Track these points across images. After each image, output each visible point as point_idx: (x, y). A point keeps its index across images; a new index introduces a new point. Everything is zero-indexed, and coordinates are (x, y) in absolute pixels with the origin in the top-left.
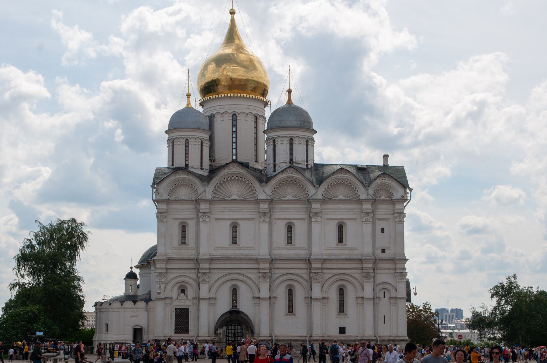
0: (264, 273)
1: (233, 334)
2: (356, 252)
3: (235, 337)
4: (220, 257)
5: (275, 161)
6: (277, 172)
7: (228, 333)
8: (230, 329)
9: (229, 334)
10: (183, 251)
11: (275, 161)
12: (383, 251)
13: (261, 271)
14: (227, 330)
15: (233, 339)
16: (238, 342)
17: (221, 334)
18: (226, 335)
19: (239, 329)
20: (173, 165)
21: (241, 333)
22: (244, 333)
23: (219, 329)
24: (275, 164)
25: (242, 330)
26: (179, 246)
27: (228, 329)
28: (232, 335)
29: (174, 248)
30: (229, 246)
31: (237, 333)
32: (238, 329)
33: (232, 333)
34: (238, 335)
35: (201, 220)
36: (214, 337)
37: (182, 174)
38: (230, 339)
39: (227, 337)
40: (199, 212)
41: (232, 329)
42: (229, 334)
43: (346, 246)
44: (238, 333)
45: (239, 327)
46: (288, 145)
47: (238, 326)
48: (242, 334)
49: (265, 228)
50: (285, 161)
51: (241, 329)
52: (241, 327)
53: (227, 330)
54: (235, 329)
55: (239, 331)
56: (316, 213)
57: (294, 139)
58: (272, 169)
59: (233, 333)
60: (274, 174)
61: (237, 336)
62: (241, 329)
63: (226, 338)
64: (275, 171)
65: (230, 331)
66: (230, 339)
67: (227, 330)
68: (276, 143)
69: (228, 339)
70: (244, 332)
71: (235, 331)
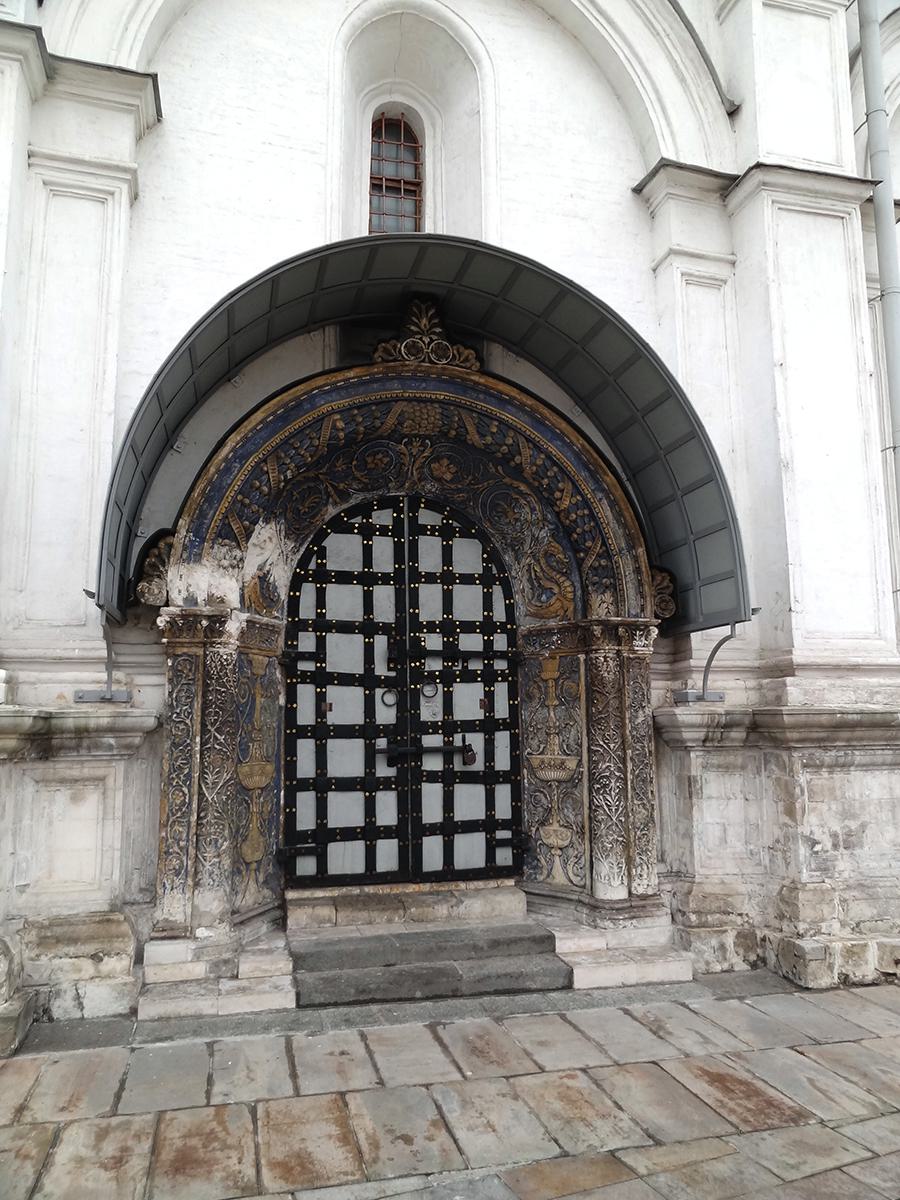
1: (381, 642)
3: (406, 685)
7: (322, 625)
8: (344, 578)
9: (332, 639)
14: (308, 592)
15: (386, 715)
16: (447, 752)
17: (218, 621)
18: (289, 661)
19: (468, 579)
21: (487, 627)
22: (525, 624)
23: (194, 555)
25: (497, 591)
27: (313, 572)
28: (369, 650)
31: (431, 627)
32: (447, 578)
33: (368, 628)
34: (450, 653)
36: (93, 678)
38: (346, 706)
39: (305, 678)
41: (368, 579)
42: (332, 639)
44: (449, 628)
45: (468, 556)
47: (446, 533)
48: (500, 642)
51: (486, 580)
52: (491, 557)
53: (308, 592)
54: (406, 579)
55: (468, 603)
59: (385, 629)
61: (435, 665)
62: (486, 580)
63: (292, 696)
65: (344, 602)
66: (346, 706)
67: (296, 583)
69: (321, 706)
70: (520, 611)
71: (406, 601)
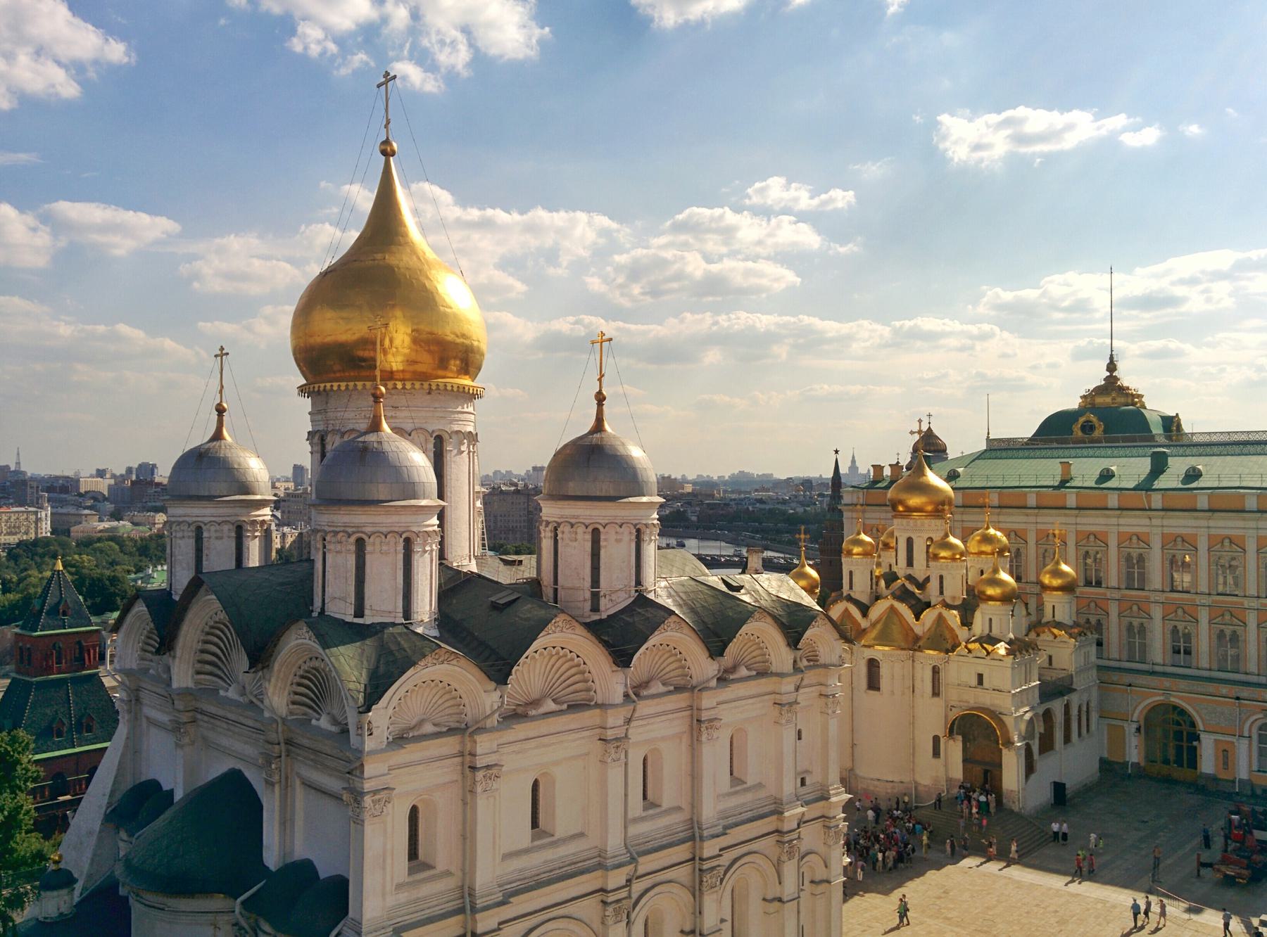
0: (618, 901)
2: (762, 794)
4: (518, 883)
5: (595, 581)
6: (604, 616)
10: (426, 890)
11: (595, 581)
12: (803, 782)
13: (609, 900)
20: (359, 612)
24: (599, 592)
26: (411, 879)
29: (399, 887)
30: (530, 845)
35: (479, 789)
37: (435, 662)
40: (473, 768)
43: (745, 786)
46: (633, 545)
49: (615, 774)
50: (626, 586)
56: (711, 720)
57: (643, 529)
58: (588, 605)
60: (596, 617)
64: (595, 608)
68: (602, 537)
